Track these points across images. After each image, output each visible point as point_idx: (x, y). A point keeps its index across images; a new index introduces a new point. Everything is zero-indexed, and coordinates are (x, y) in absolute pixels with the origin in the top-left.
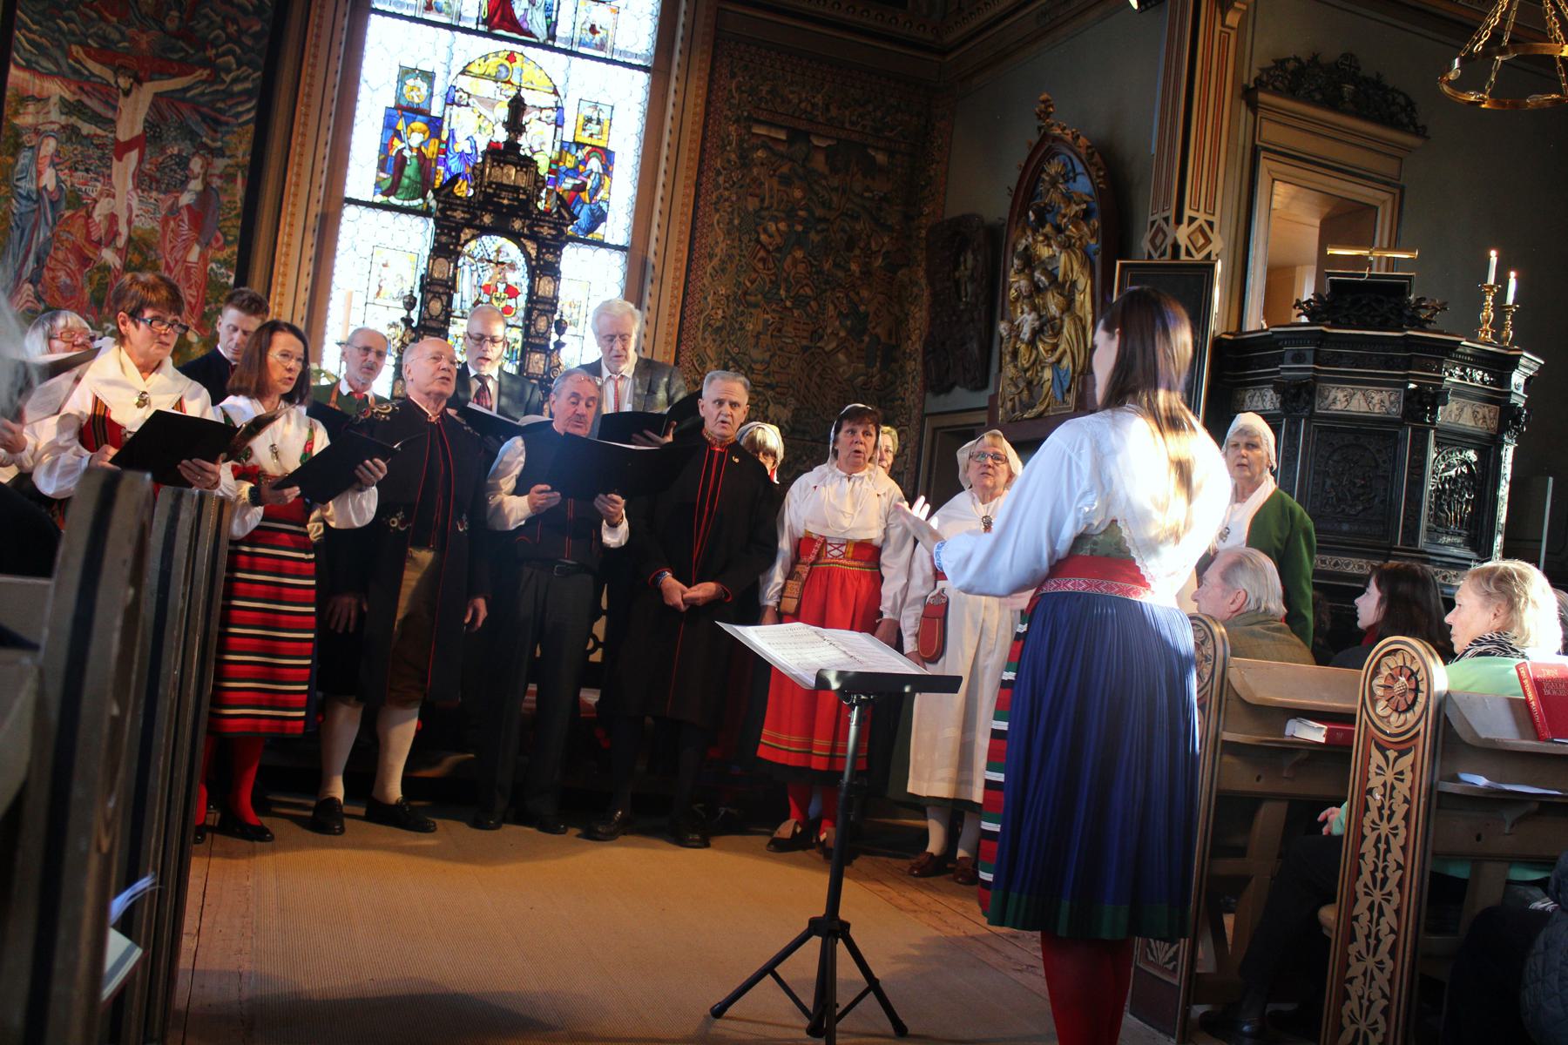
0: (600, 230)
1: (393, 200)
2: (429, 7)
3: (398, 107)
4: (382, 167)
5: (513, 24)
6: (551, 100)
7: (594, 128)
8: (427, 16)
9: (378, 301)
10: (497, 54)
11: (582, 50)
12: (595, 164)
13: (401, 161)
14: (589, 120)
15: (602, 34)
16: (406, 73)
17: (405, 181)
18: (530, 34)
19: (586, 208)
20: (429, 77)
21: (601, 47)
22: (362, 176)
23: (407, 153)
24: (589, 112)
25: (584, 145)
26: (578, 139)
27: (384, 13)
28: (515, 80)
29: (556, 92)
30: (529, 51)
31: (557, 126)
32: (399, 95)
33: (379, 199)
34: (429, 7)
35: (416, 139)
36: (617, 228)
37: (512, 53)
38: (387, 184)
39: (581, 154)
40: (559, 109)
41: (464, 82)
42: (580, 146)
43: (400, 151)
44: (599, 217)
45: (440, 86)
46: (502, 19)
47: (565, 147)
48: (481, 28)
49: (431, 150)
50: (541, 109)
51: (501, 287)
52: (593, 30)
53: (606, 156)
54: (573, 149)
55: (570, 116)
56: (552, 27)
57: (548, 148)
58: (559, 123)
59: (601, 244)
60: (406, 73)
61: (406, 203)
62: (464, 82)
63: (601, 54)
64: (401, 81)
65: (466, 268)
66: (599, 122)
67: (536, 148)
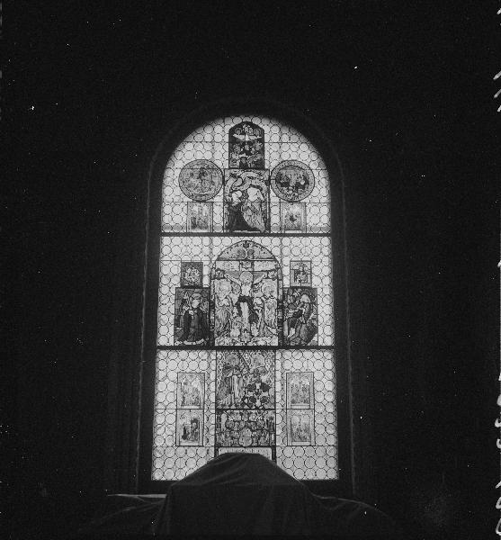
0: (315, 339)
1: (186, 343)
2: (194, 226)
3: (183, 287)
4: (177, 323)
5: (244, 225)
6: (271, 266)
8: (194, 231)
9: (185, 407)
10: (237, 244)
11: (287, 232)
12: (305, 298)
13: (188, 317)
14: (298, 272)
15: (298, 220)
16: (185, 266)
17: (192, 330)
18: (255, 229)
20: (199, 266)
21: (296, 229)
22: (166, 334)
23: (191, 312)
25: (297, 288)
26: (293, 285)
27: (169, 235)
29: (276, 261)
30: (257, 240)
32: (182, 280)
33: (178, 343)
34: (194, 226)
35: (196, 304)
36: (325, 335)
37: (246, 241)
38: (182, 333)
39: (295, 294)
41: (220, 265)
42: (294, 289)
43: (187, 312)
44: (313, 331)
45: (206, 271)
46: (238, 224)
49: (205, 308)
50: (268, 272)
51: (258, 386)
52: (292, 219)
53: (311, 292)
55: (286, 271)
56: (267, 221)
57: (276, 296)
58: (279, 279)
59: (318, 348)
60: (185, 266)
61: (194, 343)
62: (220, 265)
64: (183, 271)
65: (235, 377)
67: (268, 295)
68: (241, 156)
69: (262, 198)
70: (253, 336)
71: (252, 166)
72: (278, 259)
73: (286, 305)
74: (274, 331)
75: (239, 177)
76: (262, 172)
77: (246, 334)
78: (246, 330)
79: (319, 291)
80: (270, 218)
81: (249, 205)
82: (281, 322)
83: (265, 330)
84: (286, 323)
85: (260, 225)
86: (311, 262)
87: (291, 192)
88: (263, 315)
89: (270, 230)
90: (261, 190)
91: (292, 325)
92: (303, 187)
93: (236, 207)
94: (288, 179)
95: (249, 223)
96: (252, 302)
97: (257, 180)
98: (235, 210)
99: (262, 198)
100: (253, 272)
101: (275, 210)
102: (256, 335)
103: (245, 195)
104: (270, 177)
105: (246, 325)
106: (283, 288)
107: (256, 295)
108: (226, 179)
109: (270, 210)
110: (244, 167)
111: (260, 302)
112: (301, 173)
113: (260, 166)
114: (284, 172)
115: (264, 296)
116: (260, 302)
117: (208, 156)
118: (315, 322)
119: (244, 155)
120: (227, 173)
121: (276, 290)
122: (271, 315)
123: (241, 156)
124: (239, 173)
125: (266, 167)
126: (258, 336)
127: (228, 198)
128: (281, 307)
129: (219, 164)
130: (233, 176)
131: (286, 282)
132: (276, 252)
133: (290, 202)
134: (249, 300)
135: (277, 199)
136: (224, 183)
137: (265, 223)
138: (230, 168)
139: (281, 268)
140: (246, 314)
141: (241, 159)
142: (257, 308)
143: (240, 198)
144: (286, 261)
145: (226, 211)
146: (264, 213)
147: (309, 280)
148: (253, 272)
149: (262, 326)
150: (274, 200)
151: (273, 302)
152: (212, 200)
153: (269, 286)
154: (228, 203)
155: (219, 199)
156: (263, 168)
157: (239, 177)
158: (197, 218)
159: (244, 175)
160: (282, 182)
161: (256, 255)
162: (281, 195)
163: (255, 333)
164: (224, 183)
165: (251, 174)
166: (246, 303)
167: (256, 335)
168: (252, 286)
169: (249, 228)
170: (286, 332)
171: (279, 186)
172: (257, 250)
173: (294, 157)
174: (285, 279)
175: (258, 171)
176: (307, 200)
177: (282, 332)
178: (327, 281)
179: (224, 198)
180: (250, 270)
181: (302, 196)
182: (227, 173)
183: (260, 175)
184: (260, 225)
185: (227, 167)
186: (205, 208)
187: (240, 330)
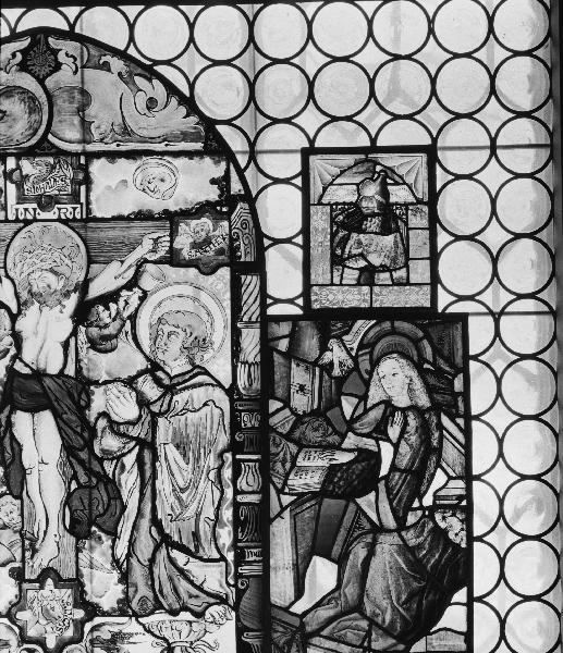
6: (194, 181)
7: (380, 247)
12: (396, 380)
14: (350, 219)
19: (387, 546)
24: (343, 194)
25: (350, 315)
26: (326, 298)
28: (68, 134)
29: (216, 148)
31: (239, 270)
37: (40, 35)
39: (336, 354)
40: (231, 201)
42: (330, 322)
47: (274, 345)
50: (172, 219)
53: (436, 340)
54: (310, 344)
55: (280, 211)
57: (221, 367)
58: (244, 262)
66: (390, 218)
67: (177, 366)
70: (93, 610)
72: (236, 142)
73: (281, 420)
74: (213, 577)
77: (54, 597)
78: (47, 572)
79: (479, 333)
82: (253, 525)
83: (161, 570)
84: (281, 531)
86: (431, 152)
88: (148, 482)
91: (318, 543)
96: (81, 409)
100: (85, 223)
102: (108, 603)
105: (53, 548)
106: (266, 321)
107: (101, 365)
111: (126, 409)
115: (154, 368)
116: (126, 409)
118: (453, 525)
121: (221, 334)
122: (192, 489)
126: (123, 608)
128: (254, 436)
131: (283, 276)
132: (220, 95)
134: (66, 396)
139: (249, 199)
140: (48, 483)
142: (111, 442)
144: (280, 153)
147: (420, 271)
148: (85, 223)
149: (145, 547)
151: (204, 412)
153: (187, 308)
161: (102, 116)
163: (105, 588)
166: (46, 417)
167: (108, 603)
168: (82, 315)
170: (281, 587)
172: (105, 85)
174: (273, 257)
177: (264, 580)
178: (526, 267)
180: (67, 210)
187: (18, 575)
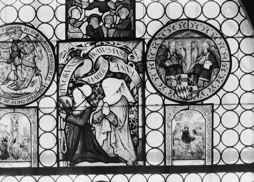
5: (98, 153)
11: (177, 163)
15: (198, 140)
18: (117, 159)
21: (199, 155)
46: (85, 149)
48: (62, 164)
52: (186, 137)
56: (140, 145)
63: (201, 163)
68: (89, 13)
69: (131, 99)
71: (112, 32)
75: (86, 56)
76: (131, 45)
80: (144, 136)
81: (106, 111)
85: (127, 152)
87: (185, 84)
89: (145, 160)
90: (128, 82)
92: (208, 74)
93: (81, 116)
94: (179, 57)
95: (105, 148)
97: (121, 63)
98: (80, 122)
99: (131, 99)
101: (154, 121)
103: (98, 92)
104: (144, 55)
108: (62, 61)
109: (144, 118)
110: (95, 37)
112: (205, 45)
113: (126, 32)
114: (173, 45)
117: (27, 16)
119: (96, 11)
120: (64, 48)
123: (89, 13)
124: (87, 47)
125: (138, 35)
127: (65, 99)
129: (47, 31)
130: (74, 54)
133: (182, 103)
135: (158, 100)
136: (58, 69)
137: (135, 147)
138: (68, 40)
141: (89, 19)
143: (88, 99)
145: (62, 125)
146: (132, 127)
150: (153, 100)
152: (35, 104)
154: (64, 109)
155: (48, 103)
156: (132, 37)
157: (86, 56)
158: (10, 139)
159: (98, 52)
160: (171, 66)
162: (166, 91)
164: (58, 69)
165: (108, 49)
169: (107, 158)
171: (162, 70)
173: (192, 12)
175: (122, 44)
176: (215, 100)
179: (59, 101)
181: (206, 92)
182: (64, 48)
183: (126, 50)
184: (127, 152)
185: (63, 38)
186: (24, 121)
